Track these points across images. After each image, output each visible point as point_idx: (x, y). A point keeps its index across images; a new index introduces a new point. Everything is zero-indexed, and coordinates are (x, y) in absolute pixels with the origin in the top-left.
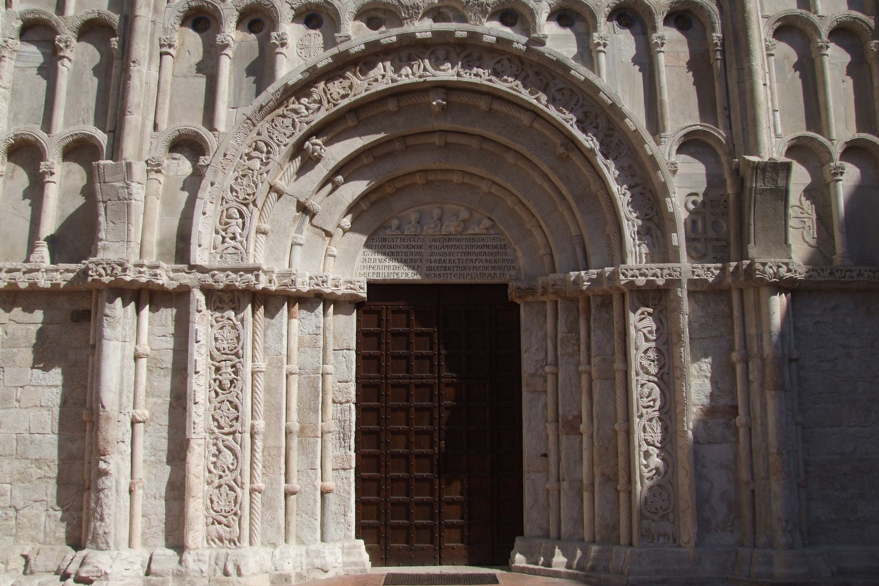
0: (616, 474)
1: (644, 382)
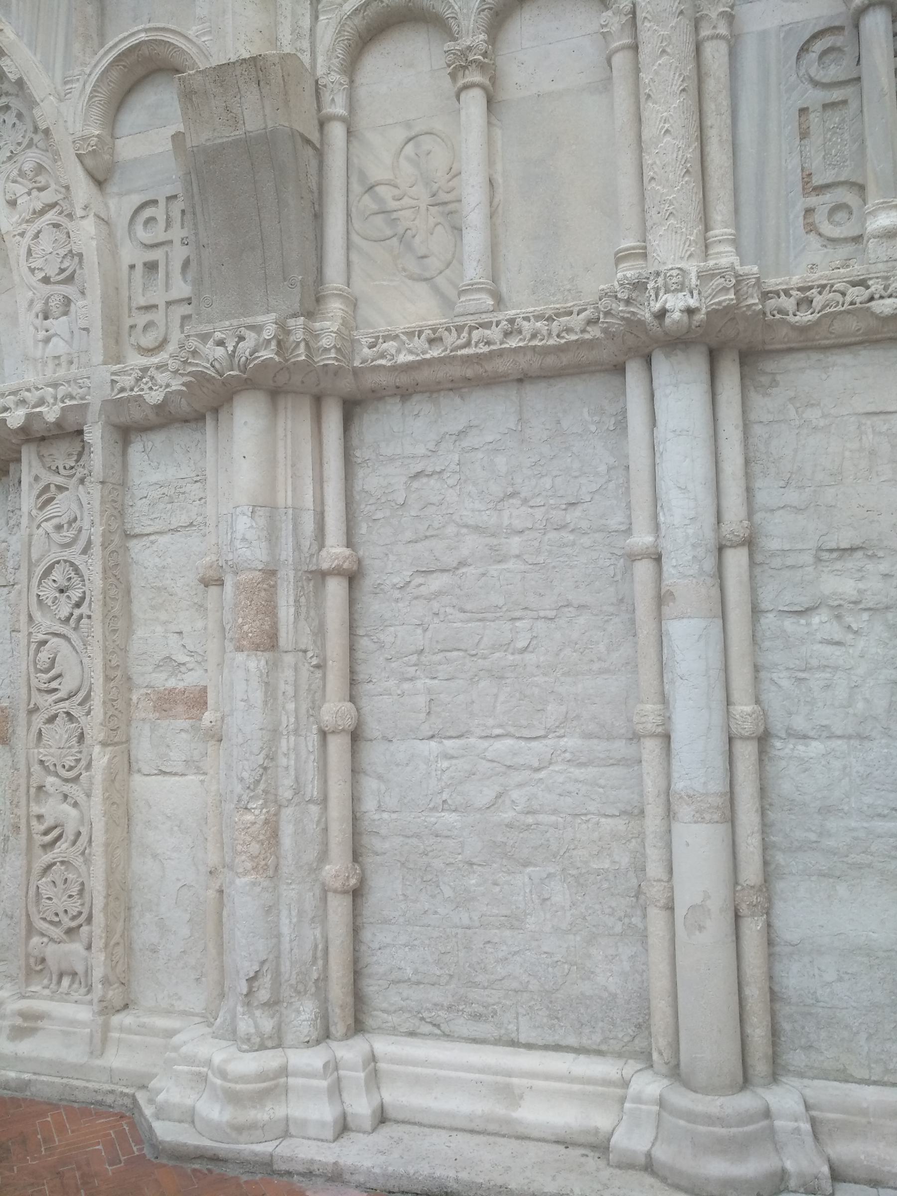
1: (41, 637)
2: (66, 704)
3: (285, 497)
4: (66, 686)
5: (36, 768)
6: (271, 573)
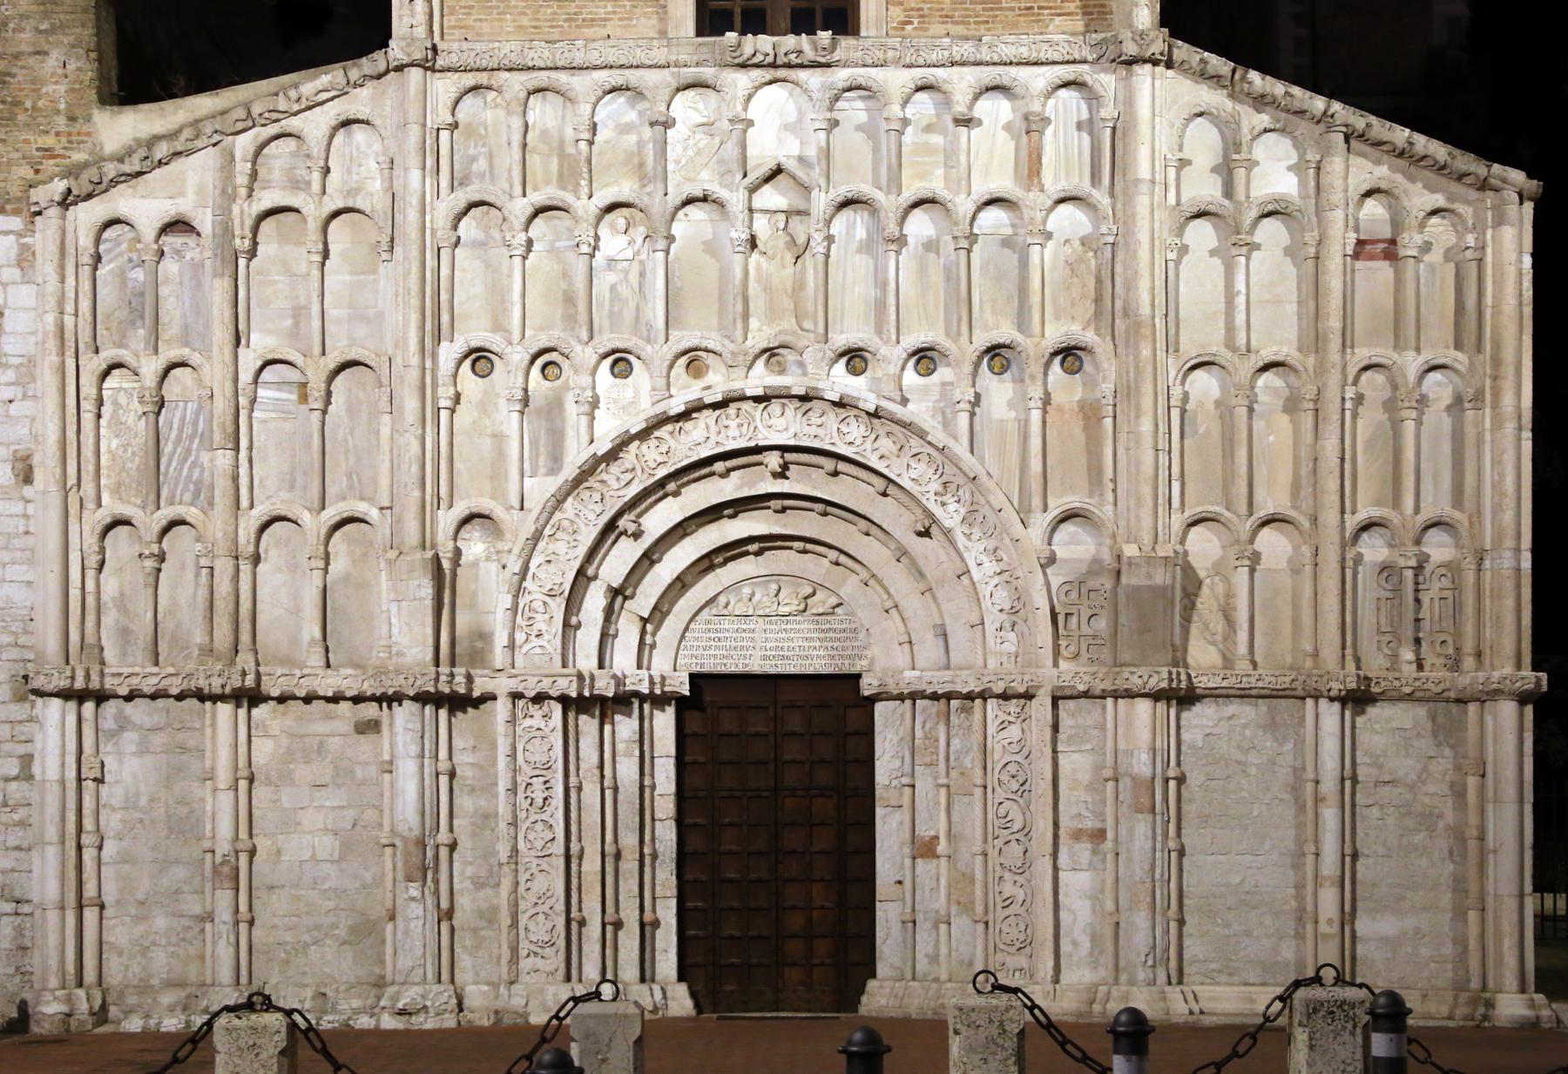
0: (973, 902)
2: (1017, 836)
3: (1158, 744)
4: (1017, 825)
5: (998, 868)
6: (1153, 779)
